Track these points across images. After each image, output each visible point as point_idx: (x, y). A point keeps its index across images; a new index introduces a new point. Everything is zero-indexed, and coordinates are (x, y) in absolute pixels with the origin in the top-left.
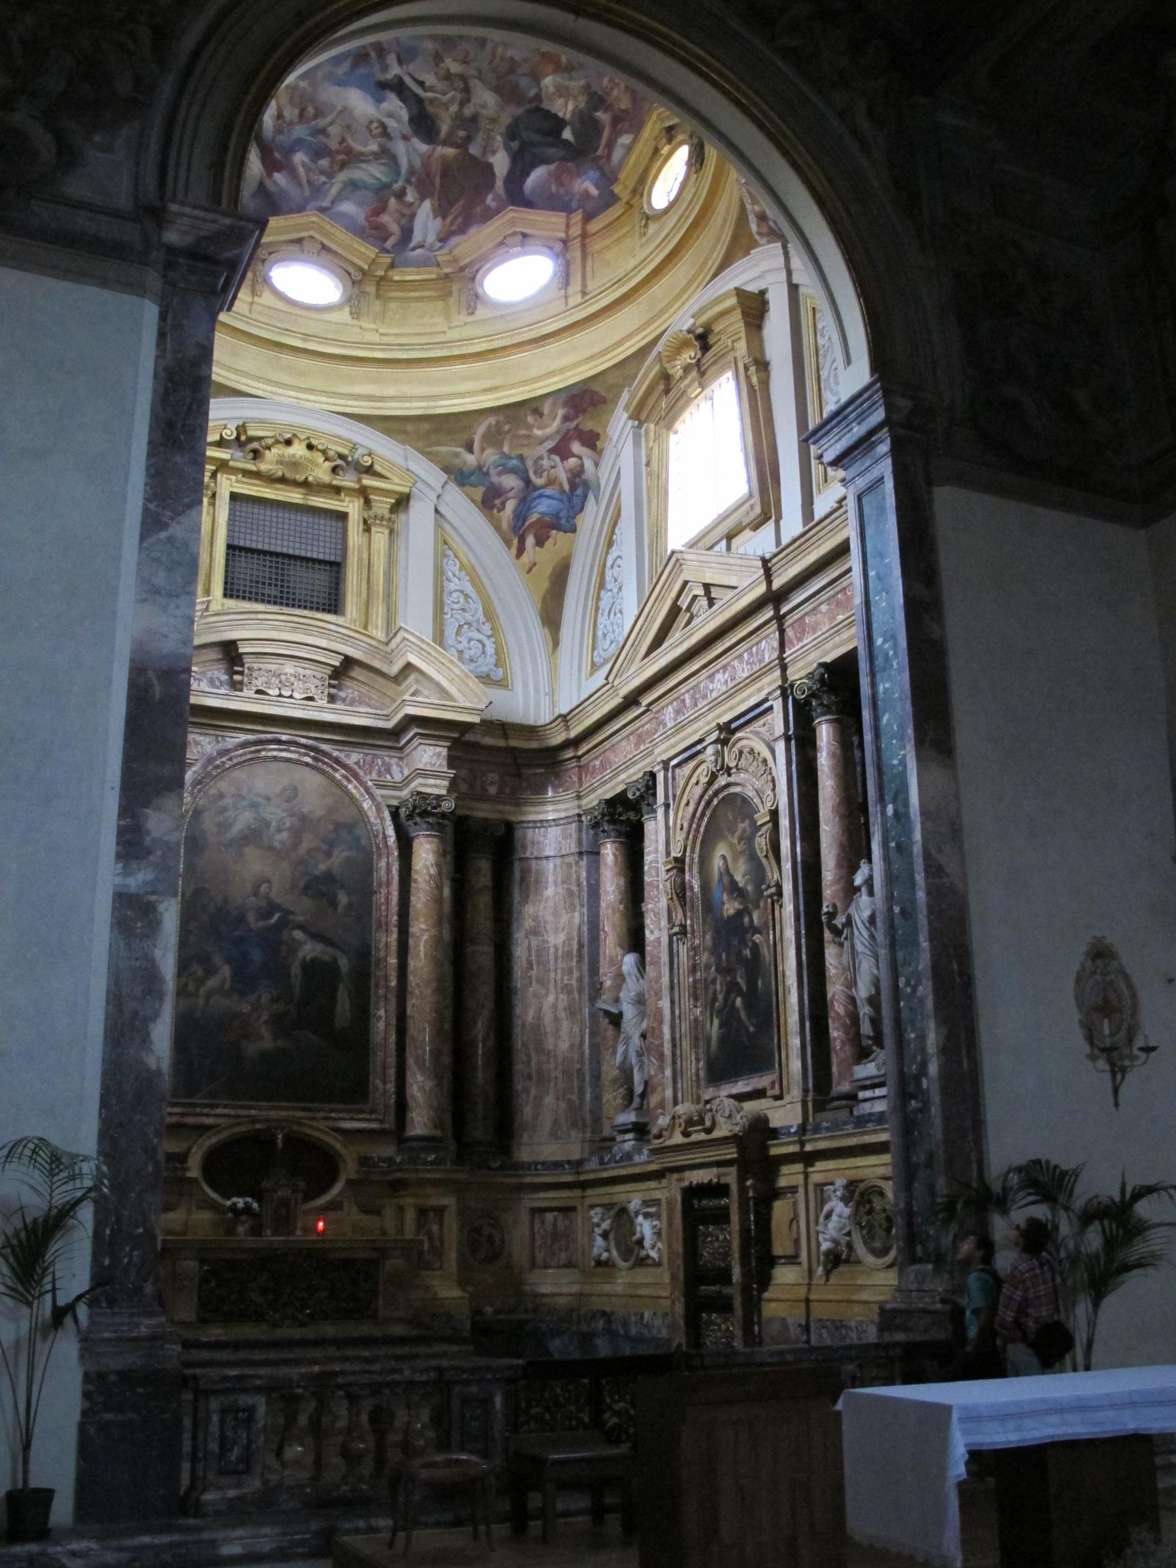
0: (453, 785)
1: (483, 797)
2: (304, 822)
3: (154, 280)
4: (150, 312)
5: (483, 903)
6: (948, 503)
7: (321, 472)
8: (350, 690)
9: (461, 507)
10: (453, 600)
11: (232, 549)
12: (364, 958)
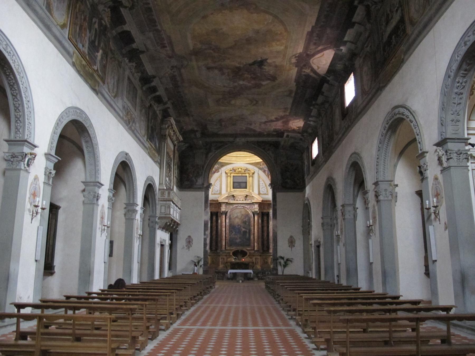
0: (259, 209)
1: (265, 209)
2: (242, 215)
3: (204, 190)
4: (204, 193)
5: (265, 222)
6: (278, 195)
7: (243, 171)
8: (248, 198)
9: (261, 173)
10: (261, 185)
11: (234, 182)
12: (250, 231)
